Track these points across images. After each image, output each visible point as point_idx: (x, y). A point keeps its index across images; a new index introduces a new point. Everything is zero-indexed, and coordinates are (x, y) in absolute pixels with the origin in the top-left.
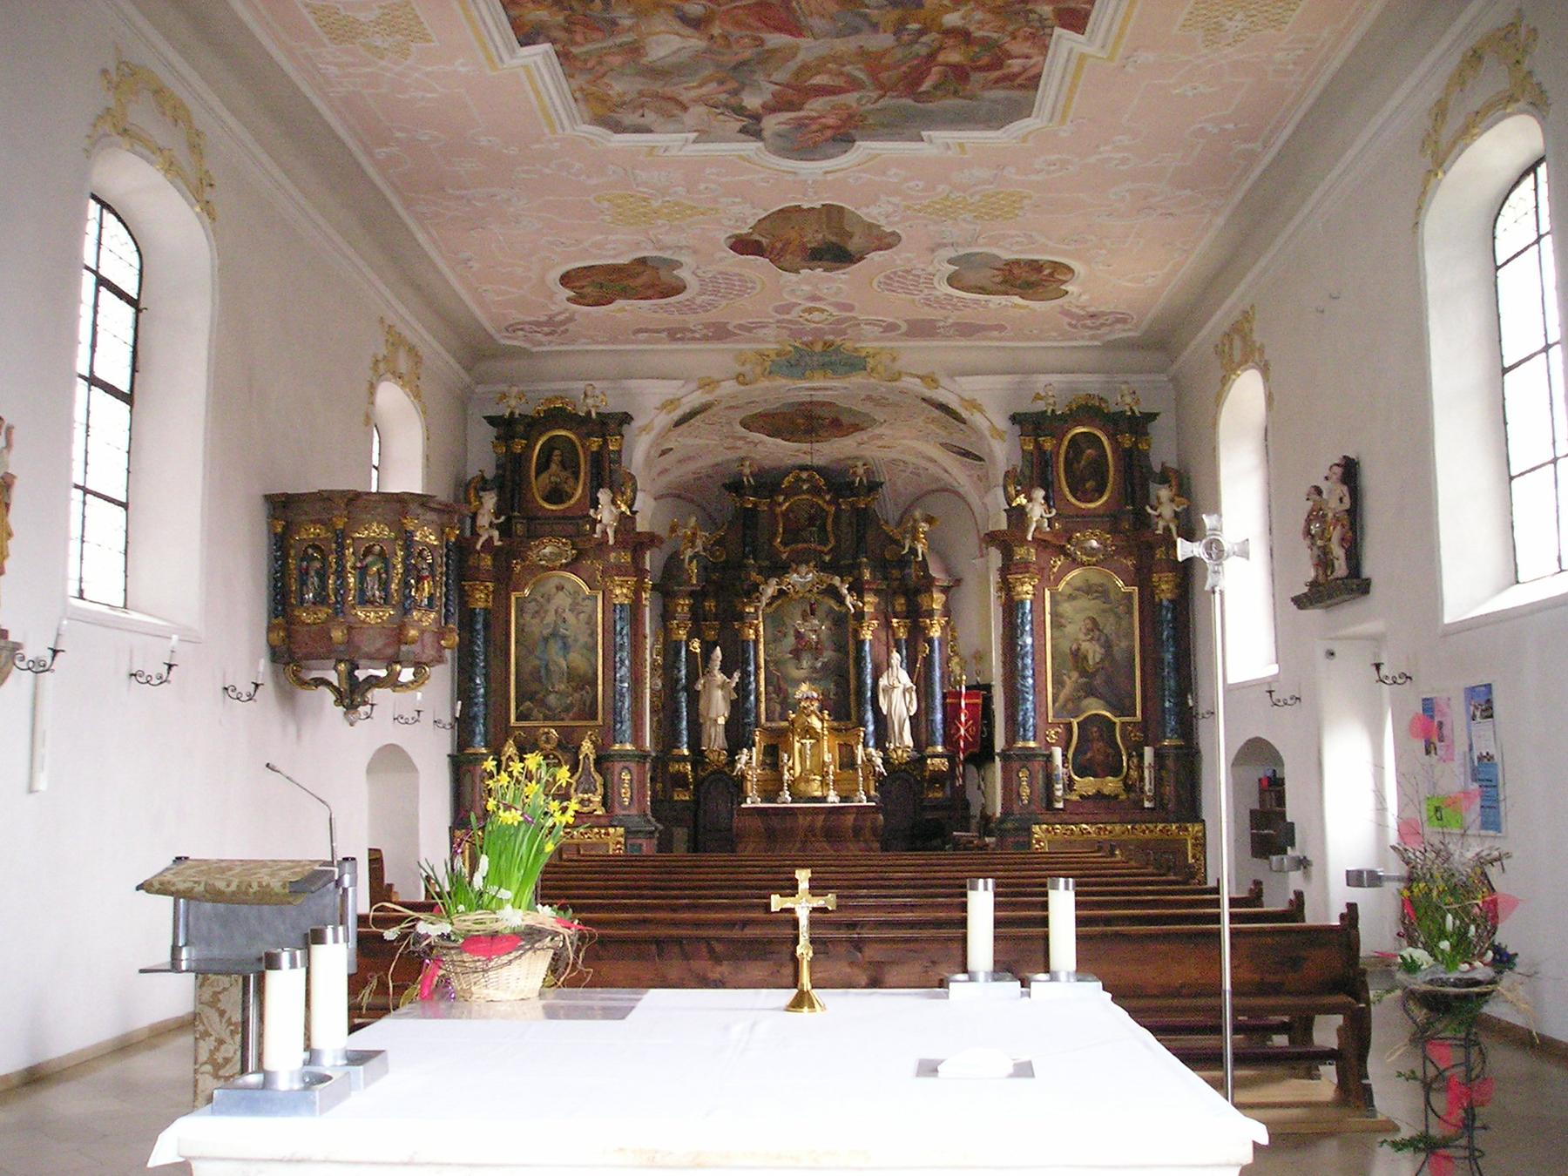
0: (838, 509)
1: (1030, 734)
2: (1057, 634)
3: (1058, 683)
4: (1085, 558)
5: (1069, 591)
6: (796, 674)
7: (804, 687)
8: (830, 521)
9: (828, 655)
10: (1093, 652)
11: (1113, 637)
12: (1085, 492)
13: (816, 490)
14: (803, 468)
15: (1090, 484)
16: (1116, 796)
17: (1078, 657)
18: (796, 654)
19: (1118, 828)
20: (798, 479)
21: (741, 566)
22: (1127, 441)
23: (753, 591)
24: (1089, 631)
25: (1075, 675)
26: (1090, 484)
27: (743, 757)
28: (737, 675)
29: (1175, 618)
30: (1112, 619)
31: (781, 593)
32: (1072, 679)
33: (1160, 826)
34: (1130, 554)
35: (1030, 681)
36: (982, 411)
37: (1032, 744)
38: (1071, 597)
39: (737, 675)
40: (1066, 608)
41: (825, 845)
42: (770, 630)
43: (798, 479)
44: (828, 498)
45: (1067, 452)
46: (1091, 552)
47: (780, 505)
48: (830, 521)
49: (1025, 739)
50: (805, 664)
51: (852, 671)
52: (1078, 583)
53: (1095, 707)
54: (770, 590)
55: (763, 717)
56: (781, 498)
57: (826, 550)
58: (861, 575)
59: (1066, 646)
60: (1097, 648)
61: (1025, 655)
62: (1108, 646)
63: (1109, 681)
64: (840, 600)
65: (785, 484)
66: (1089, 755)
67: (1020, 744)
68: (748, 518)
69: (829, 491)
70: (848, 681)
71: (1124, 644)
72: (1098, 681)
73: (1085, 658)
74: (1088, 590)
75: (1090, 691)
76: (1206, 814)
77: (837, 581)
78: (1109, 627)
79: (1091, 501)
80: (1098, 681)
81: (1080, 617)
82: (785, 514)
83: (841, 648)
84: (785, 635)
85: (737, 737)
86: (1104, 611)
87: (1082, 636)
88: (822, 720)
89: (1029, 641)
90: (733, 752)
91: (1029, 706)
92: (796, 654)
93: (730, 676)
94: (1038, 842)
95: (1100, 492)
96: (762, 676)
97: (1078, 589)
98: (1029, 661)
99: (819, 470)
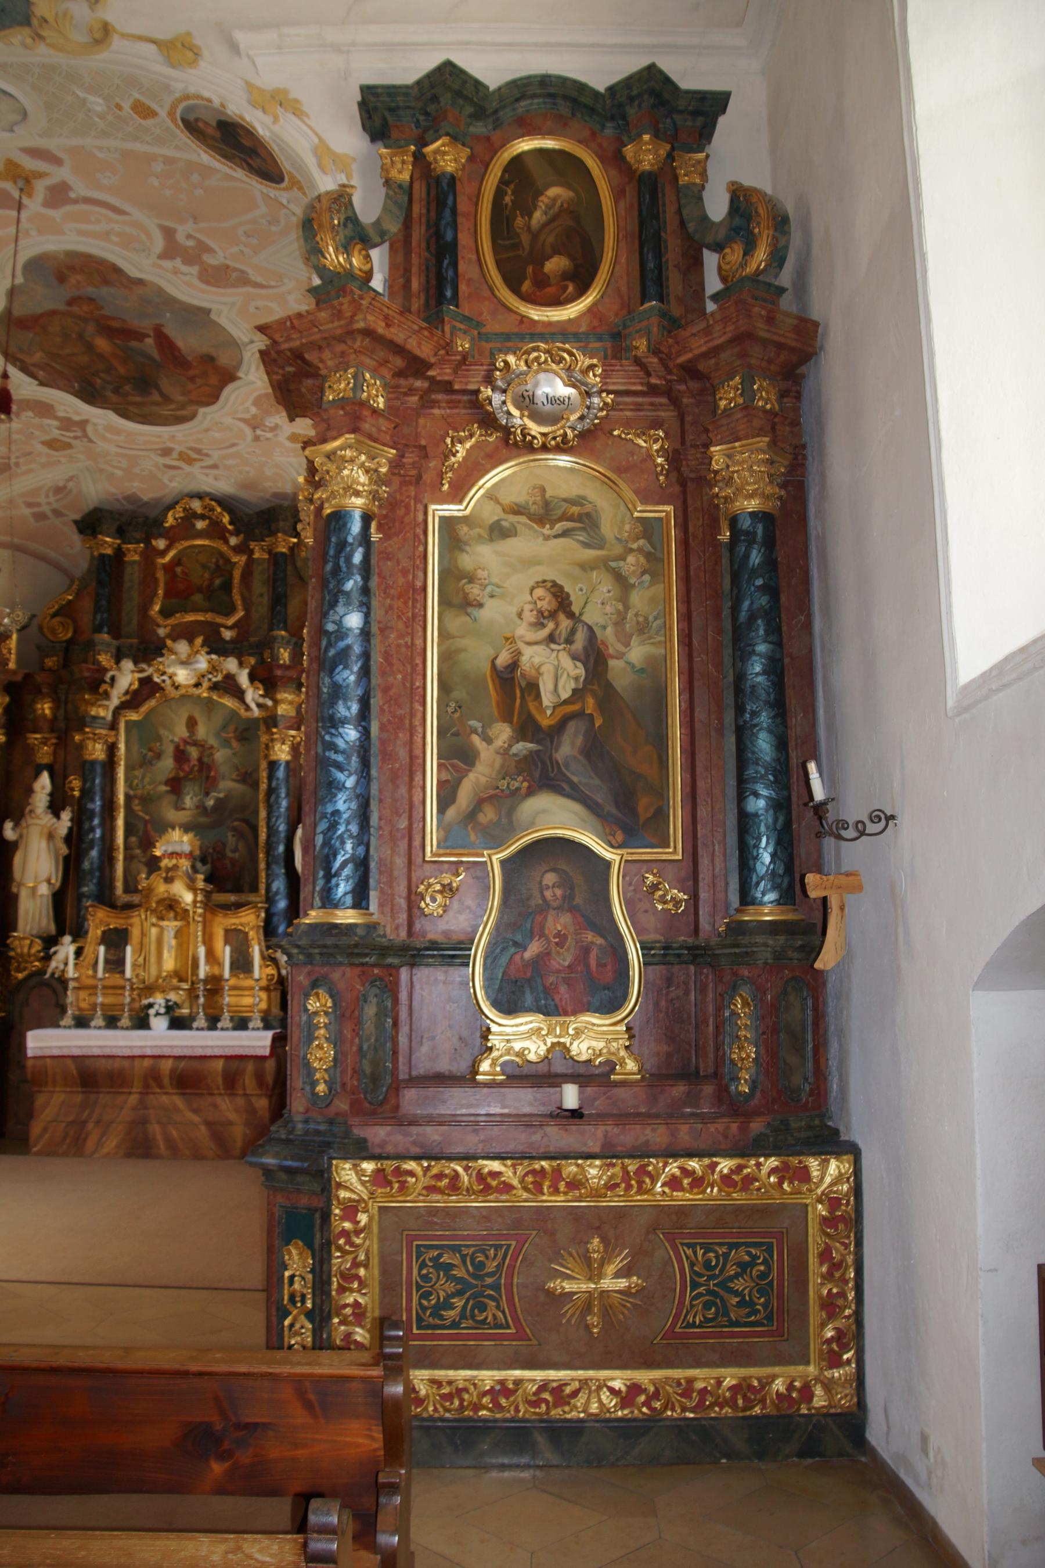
0: (250, 562)
1: (343, 888)
2: (457, 622)
3: (457, 755)
4: (535, 429)
5: (492, 514)
6: (172, 815)
7: (176, 835)
8: (237, 574)
9: (227, 785)
10: (556, 674)
11: (608, 635)
12: (541, 281)
13: (216, 531)
14: (200, 496)
15: (555, 265)
16: (611, 1066)
17: (512, 685)
18: (175, 785)
19: (594, 1171)
20: (191, 516)
21: (90, 645)
22: (645, 154)
23: (97, 684)
24: (542, 618)
25: (503, 733)
26: (555, 265)
27: (67, 948)
28: (66, 816)
29: (771, 564)
30: (606, 587)
31: (147, 688)
32: (496, 743)
33: (725, 1165)
34: (657, 424)
35: (351, 734)
36: (297, 111)
37: (347, 916)
38: (499, 532)
39: (66, 816)
40: (484, 557)
41: (178, 1101)
42: (135, 747)
43: (191, 516)
44: (233, 541)
45: (499, 194)
46: (550, 414)
47: (163, 553)
48: (237, 574)
49: (328, 901)
50: (188, 801)
51: (263, 814)
52: (518, 495)
53: (556, 818)
54: (126, 677)
55: (119, 885)
56: (161, 544)
57: (230, 622)
58: (275, 657)
59: (479, 656)
60: (566, 662)
61: (343, 656)
62: (594, 658)
63: (594, 750)
64: (239, 694)
65: (170, 521)
66: (534, 949)
67: (313, 916)
68: (108, 571)
69: (236, 533)
70: (255, 829)
71: (637, 653)
72: (567, 748)
73: (533, 688)
74: (545, 513)
75: (542, 775)
76: (858, 1124)
77: (231, 664)
78: (597, 606)
79: (557, 302)
80: (567, 748)
81: (519, 583)
82: (168, 568)
83: (248, 778)
84: (159, 756)
85: (66, 917)
86: (586, 567)
87: (523, 631)
88: (192, 888)
89: (354, 620)
90: (51, 941)
91: (343, 804)
92: (175, 785)
93: (57, 816)
94: (351, 1210)
95: (581, 279)
96: (120, 822)
97: (517, 510)
98: (349, 676)
99: (225, 502)
